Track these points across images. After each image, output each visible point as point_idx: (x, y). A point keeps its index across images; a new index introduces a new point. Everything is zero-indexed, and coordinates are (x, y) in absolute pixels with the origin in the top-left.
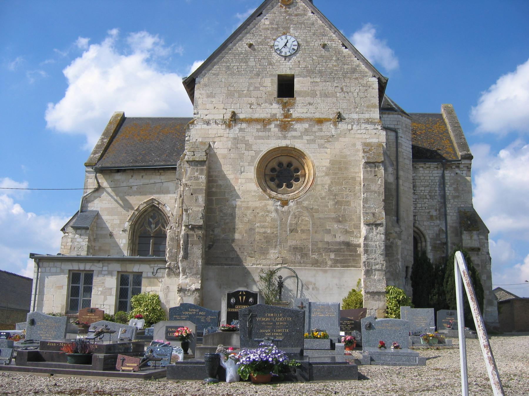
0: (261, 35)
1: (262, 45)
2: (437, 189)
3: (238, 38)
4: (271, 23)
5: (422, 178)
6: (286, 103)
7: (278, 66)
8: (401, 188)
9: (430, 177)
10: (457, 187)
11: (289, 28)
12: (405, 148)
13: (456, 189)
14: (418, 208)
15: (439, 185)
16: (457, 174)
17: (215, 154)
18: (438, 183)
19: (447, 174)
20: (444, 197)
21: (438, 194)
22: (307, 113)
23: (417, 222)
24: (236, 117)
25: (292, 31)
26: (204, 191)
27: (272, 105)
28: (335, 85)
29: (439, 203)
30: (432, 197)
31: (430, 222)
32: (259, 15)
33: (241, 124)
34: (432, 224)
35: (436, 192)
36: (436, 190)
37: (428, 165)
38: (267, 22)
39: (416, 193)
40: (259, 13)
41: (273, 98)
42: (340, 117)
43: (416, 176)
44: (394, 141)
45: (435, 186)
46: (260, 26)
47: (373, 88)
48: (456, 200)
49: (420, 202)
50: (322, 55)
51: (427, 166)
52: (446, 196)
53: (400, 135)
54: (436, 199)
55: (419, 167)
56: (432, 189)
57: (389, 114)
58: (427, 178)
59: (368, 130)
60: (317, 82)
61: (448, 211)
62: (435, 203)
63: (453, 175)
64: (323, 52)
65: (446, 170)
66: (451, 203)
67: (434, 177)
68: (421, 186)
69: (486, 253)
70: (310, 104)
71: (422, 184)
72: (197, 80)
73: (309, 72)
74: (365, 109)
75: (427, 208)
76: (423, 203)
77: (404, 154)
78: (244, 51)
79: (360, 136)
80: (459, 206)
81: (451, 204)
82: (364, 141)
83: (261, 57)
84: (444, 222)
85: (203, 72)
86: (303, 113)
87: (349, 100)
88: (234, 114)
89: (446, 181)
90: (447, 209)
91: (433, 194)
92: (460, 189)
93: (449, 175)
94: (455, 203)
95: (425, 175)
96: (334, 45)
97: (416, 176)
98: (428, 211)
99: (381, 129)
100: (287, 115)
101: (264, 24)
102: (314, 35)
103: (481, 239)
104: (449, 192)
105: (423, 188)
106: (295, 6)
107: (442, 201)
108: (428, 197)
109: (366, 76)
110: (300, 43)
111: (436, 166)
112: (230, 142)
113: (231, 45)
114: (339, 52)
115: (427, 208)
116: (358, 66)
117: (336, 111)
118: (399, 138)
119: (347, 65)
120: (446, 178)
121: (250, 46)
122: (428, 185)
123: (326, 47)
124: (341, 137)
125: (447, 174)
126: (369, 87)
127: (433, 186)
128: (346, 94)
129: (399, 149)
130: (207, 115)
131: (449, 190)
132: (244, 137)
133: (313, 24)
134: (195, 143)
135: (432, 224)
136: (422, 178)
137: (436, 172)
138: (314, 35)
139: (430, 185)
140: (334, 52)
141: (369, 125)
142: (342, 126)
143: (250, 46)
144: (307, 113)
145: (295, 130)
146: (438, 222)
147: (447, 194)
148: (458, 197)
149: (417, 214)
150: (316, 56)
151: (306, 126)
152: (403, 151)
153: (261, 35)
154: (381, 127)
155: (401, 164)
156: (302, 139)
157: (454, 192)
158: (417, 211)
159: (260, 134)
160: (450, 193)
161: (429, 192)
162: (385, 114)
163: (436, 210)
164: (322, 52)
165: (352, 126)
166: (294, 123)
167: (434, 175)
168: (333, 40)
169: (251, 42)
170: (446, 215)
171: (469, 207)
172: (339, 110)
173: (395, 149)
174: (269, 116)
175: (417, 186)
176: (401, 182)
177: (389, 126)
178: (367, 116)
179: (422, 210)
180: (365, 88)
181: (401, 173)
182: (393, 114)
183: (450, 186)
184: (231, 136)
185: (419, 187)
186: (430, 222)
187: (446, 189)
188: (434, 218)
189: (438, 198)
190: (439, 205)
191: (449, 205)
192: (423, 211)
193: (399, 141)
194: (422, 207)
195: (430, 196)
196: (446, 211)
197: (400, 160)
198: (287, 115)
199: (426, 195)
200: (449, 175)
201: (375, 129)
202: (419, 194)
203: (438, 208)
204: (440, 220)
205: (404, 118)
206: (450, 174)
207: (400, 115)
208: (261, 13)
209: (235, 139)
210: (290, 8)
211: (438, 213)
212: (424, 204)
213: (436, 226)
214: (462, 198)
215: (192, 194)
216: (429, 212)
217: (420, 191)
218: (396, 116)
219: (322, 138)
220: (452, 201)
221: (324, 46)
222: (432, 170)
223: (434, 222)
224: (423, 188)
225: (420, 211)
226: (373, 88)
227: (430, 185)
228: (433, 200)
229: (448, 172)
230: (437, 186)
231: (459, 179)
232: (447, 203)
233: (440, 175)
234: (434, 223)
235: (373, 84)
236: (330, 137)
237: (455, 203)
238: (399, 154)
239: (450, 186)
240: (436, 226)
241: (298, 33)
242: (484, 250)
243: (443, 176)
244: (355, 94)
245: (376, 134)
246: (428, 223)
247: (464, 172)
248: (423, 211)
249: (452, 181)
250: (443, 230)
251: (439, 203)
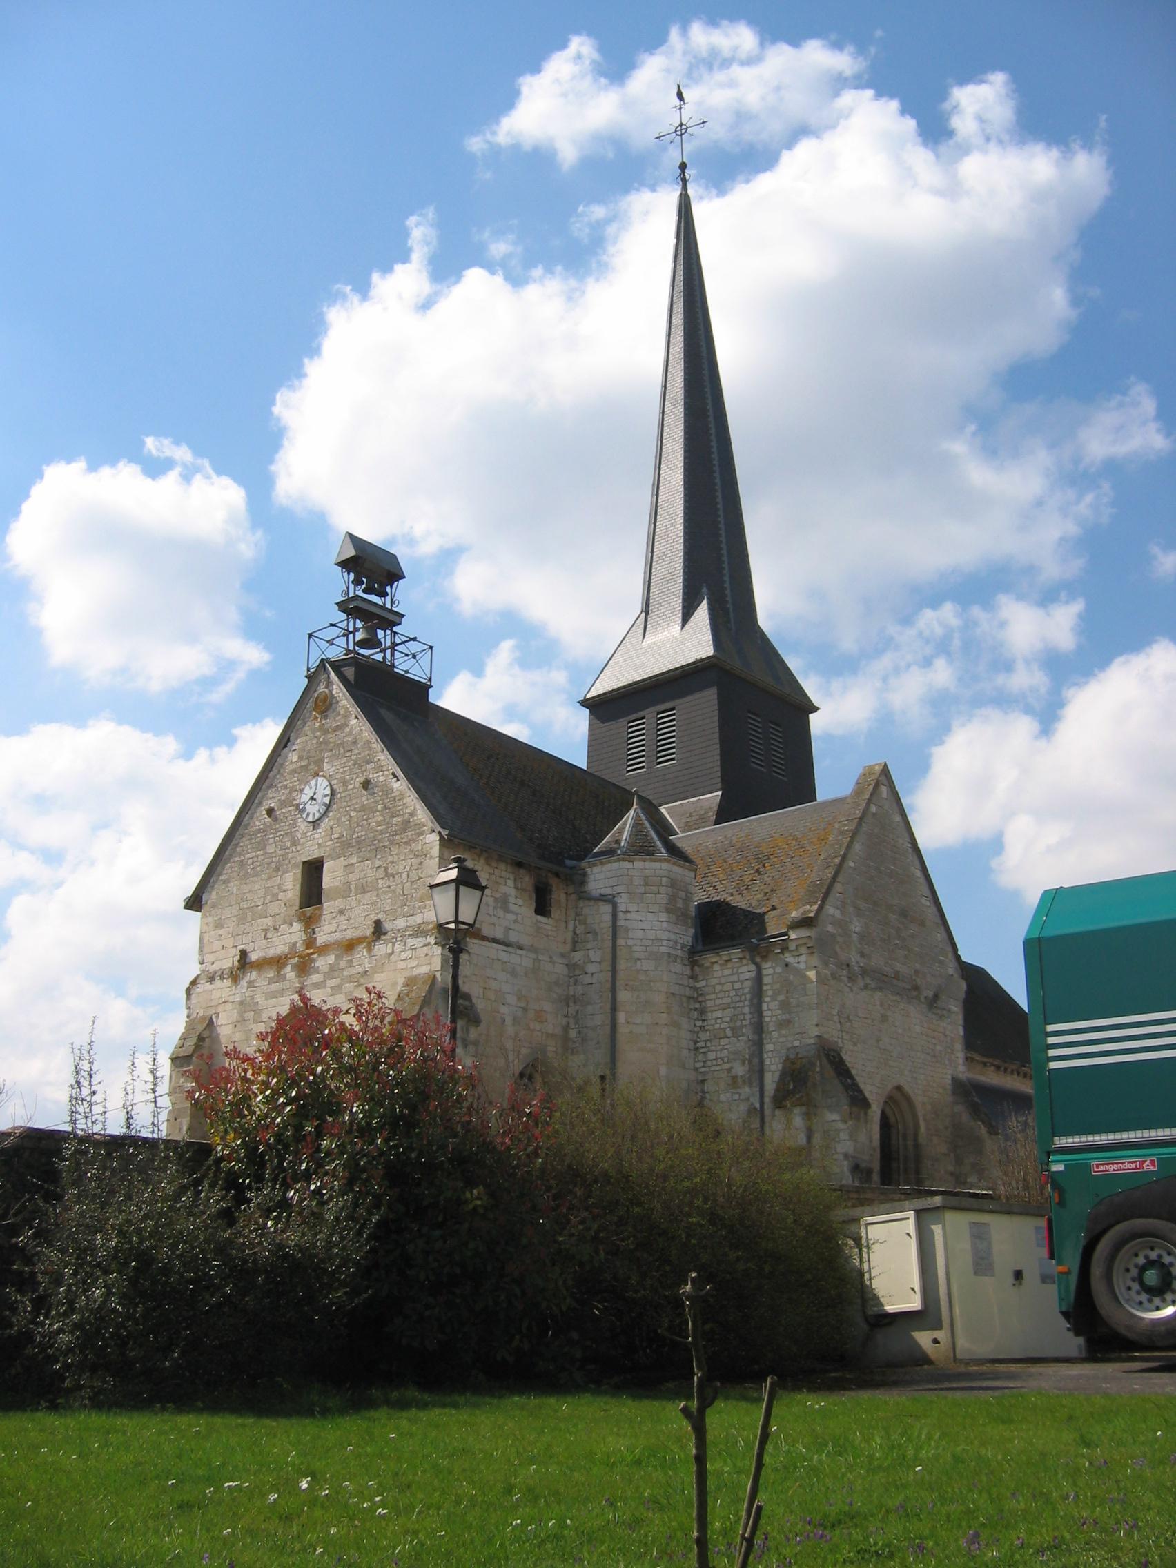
0: (285, 787)
1: (286, 807)
2: (746, 1010)
3: (257, 801)
4: (301, 758)
5: (718, 988)
6: (310, 917)
7: (304, 843)
8: (623, 1030)
9: (732, 982)
10: (787, 997)
11: (322, 760)
12: (640, 934)
13: (785, 1005)
14: (709, 1063)
15: (751, 1000)
16: (787, 965)
17: (218, 1035)
18: (748, 997)
19: (768, 969)
20: (759, 1027)
21: (747, 1022)
22: (336, 932)
23: (707, 1095)
24: (248, 960)
25: (326, 766)
26: (189, 1112)
27: (292, 925)
28: (378, 863)
29: (750, 1043)
30: (736, 1032)
31: (732, 1093)
32: (285, 746)
33: (251, 972)
34: (736, 1097)
35: (745, 1020)
36: (744, 1014)
37: (725, 954)
38: (295, 758)
39: (706, 1028)
40: (285, 740)
41: (293, 912)
42: (379, 930)
43: (707, 986)
44: (610, 924)
45: (742, 1004)
46: (285, 769)
47: (431, 857)
48: (783, 1032)
49: (713, 1048)
50: (363, 805)
51: (725, 958)
52: (764, 1024)
53: (622, 908)
54: (743, 1035)
55: (708, 964)
56: (736, 1013)
57: (602, 864)
58: (728, 987)
59: (415, 948)
60: (353, 864)
61: (767, 1062)
62: (741, 1046)
63: (779, 970)
64: (366, 799)
65: (766, 961)
66: (773, 1040)
67: (742, 982)
68: (716, 1008)
69: (841, 1157)
70: (341, 912)
71: (718, 1002)
72: (205, 897)
73: (344, 846)
74: (417, 904)
75: (726, 1060)
76: (719, 1048)
77: (635, 949)
78: (261, 827)
79: (402, 965)
80: (790, 1045)
81: (774, 1044)
82: (408, 974)
83: (282, 833)
84: (758, 1089)
85: (212, 881)
86: (332, 933)
87: (394, 891)
88: (244, 953)
89: (765, 988)
90: (765, 1056)
91: (739, 1023)
92: (793, 1001)
93: (771, 971)
94: (781, 1040)
95: (723, 980)
96: (381, 779)
97: (707, 986)
98: (726, 1066)
99: (435, 944)
100: (310, 943)
101: (292, 763)
102: (355, 765)
103: (833, 1121)
104: (769, 1013)
105: (719, 1014)
106: (333, 712)
107: (756, 1037)
108: (729, 1032)
109: (422, 834)
110: (335, 787)
111: (740, 955)
112: (235, 1011)
113: (246, 818)
114: (387, 791)
115: (726, 1060)
116: (412, 815)
117: (374, 918)
118: (621, 915)
119: (398, 816)
120: (766, 980)
121: (270, 812)
122: (729, 1004)
123: (370, 787)
124: (376, 972)
125: (768, 969)
126: (426, 855)
127: (738, 1004)
128: (391, 879)
129: (621, 942)
130: (213, 963)
131: (771, 1010)
132: (252, 998)
133: (355, 743)
134: (195, 1018)
135: (736, 1097)
136: (718, 988)
137: (744, 969)
138: (355, 765)
139: (732, 1002)
140: (380, 794)
141: (418, 939)
142: (381, 948)
143: (270, 812)
144: (336, 932)
145: (317, 971)
146: (747, 1090)
147: (767, 1019)
148: (787, 1023)
149: (706, 1078)
150: (355, 810)
151: (331, 959)
152: (630, 942)
153: (285, 787)
154: (436, 938)
155: (621, 975)
156: (325, 987)
157: (780, 1012)
158: (707, 1069)
159: (274, 987)
160: (772, 1016)
161: (731, 1021)
162: (595, 865)
163: (743, 1063)
164: (363, 799)
165: (394, 945)
166: (315, 956)
167: (742, 977)
168: (379, 769)
169: (272, 805)
170: (761, 1072)
171: (809, 1045)
172: (380, 916)
173: (610, 944)
174: (286, 949)
175: (708, 1010)
176: (621, 1017)
177: (603, 892)
178: (418, 919)
179: (717, 1065)
180: (419, 860)
181: (623, 996)
182: (610, 862)
183: (774, 999)
184: (238, 998)
185: (712, 1012)
186: (732, 1093)
187: (765, 1007)
188: (740, 1080)
189: (748, 1032)
190: (749, 1048)
191: (769, 1047)
192: (718, 1068)
193: (621, 923)
194: (716, 1059)
195: (733, 1029)
196: (762, 1062)
197: (622, 965)
198: (310, 943)
199: (724, 1029)
200: (771, 971)
201: (425, 945)
202: (711, 1028)
203: (747, 1056)
204: (751, 1085)
205: (638, 864)
206: (774, 969)
207: (624, 860)
208: (289, 741)
209: (241, 1003)
210: (326, 717)
211: (747, 1068)
212: (722, 1050)
213: (742, 1100)
214: (796, 1025)
215: (176, 1119)
216: (729, 1070)
217: (713, 1022)
218: (616, 865)
219: (350, 979)
220: (775, 1035)
221: (366, 784)
222: (737, 965)
223: (739, 1090)
224: (719, 1014)
225: (712, 1069)
226: (431, 857)
227: (732, 1002)
228: (738, 1040)
229: (769, 964)
230: (747, 1003)
231: (791, 977)
232: (765, 1041)
233: (753, 974)
234: (740, 1094)
235: (431, 848)
236: (362, 976)
237: (781, 1040)
238: (619, 953)
239: (774, 999)
240: (742, 1100)
241: (334, 768)
242: (839, 1150)
243: (759, 979)
244: (404, 875)
245: (427, 955)
246: (728, 1095)
247: (803, 958)
248: (718, 1068)
249: (777, 986)
250: (755, 1108)
251: (750, 1043)
